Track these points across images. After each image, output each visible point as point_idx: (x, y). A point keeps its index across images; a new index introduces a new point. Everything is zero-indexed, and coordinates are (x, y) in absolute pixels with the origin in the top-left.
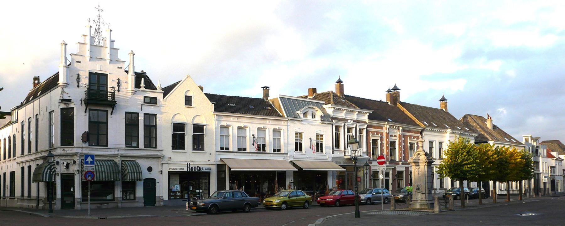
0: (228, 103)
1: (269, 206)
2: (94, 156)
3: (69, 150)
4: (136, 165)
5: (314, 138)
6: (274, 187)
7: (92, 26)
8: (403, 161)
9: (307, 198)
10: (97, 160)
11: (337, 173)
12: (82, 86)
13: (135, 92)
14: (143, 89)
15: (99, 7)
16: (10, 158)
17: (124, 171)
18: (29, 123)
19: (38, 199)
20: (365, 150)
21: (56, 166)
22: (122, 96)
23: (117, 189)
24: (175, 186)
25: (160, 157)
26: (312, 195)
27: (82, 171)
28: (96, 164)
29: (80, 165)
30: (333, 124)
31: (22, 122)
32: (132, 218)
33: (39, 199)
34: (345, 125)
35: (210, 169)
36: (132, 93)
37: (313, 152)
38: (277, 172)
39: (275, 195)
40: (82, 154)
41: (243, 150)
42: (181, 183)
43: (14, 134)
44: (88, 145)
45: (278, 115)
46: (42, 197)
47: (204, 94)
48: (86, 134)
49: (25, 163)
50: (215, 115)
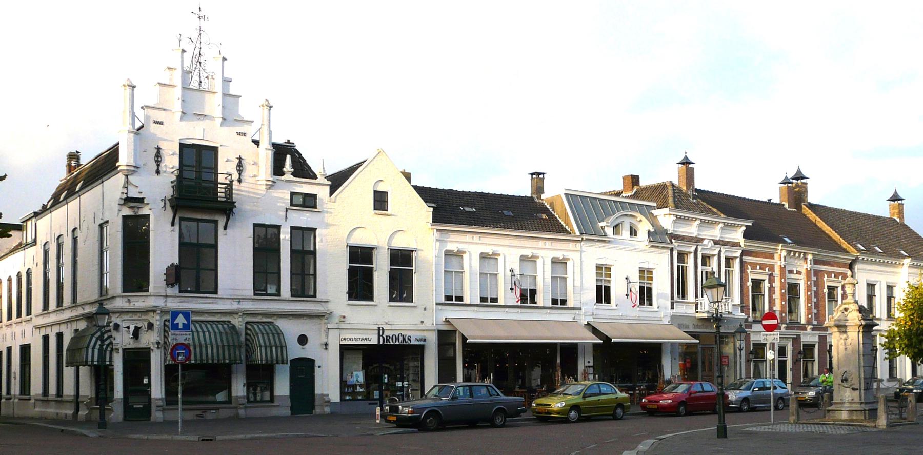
0: (461, 206)
1: (543, 415)
2: (189, 312)
3: (140, 302)
4: (274, 332)
5: (635, 277)
6: (553, 377)
7: (185, 49)
8: (815, 323)
9: (620, 398)
10: (197, 321)
11: (680, 347)
12: (165, 172)
13: (273, 184)
14: (288, 177)
15: (200, 11)
16: (21, 317)
17: (252, 344)
18: (59, 246)
19: (77, 401)
20: (737, 301)
21: (114, 334)
22: (246, 192)
23: (235, 380)
24: (355, 373)
25: (324, 316)
26: (630, 392)
27: (165, 343)
28: (194, 330)
29: (162, 331)
30: (672, 248)
31: (45, 245)
32: (266, 438)
33: (80, 399)
34: (696, 250)
35: (425, 340)
36: (266, 184)
37: (633, 305)
38: (560, 346)
39: (556, 392)
40: (166, 310)
41: (491, 302)
42: (364, 367)
43: (29, 269)
44: (178, 291)
45: (562, 230)
46: (84, 396)
47: (412, 188)
48: (174, 268)
49: (50, 327)
50: (435, 230)
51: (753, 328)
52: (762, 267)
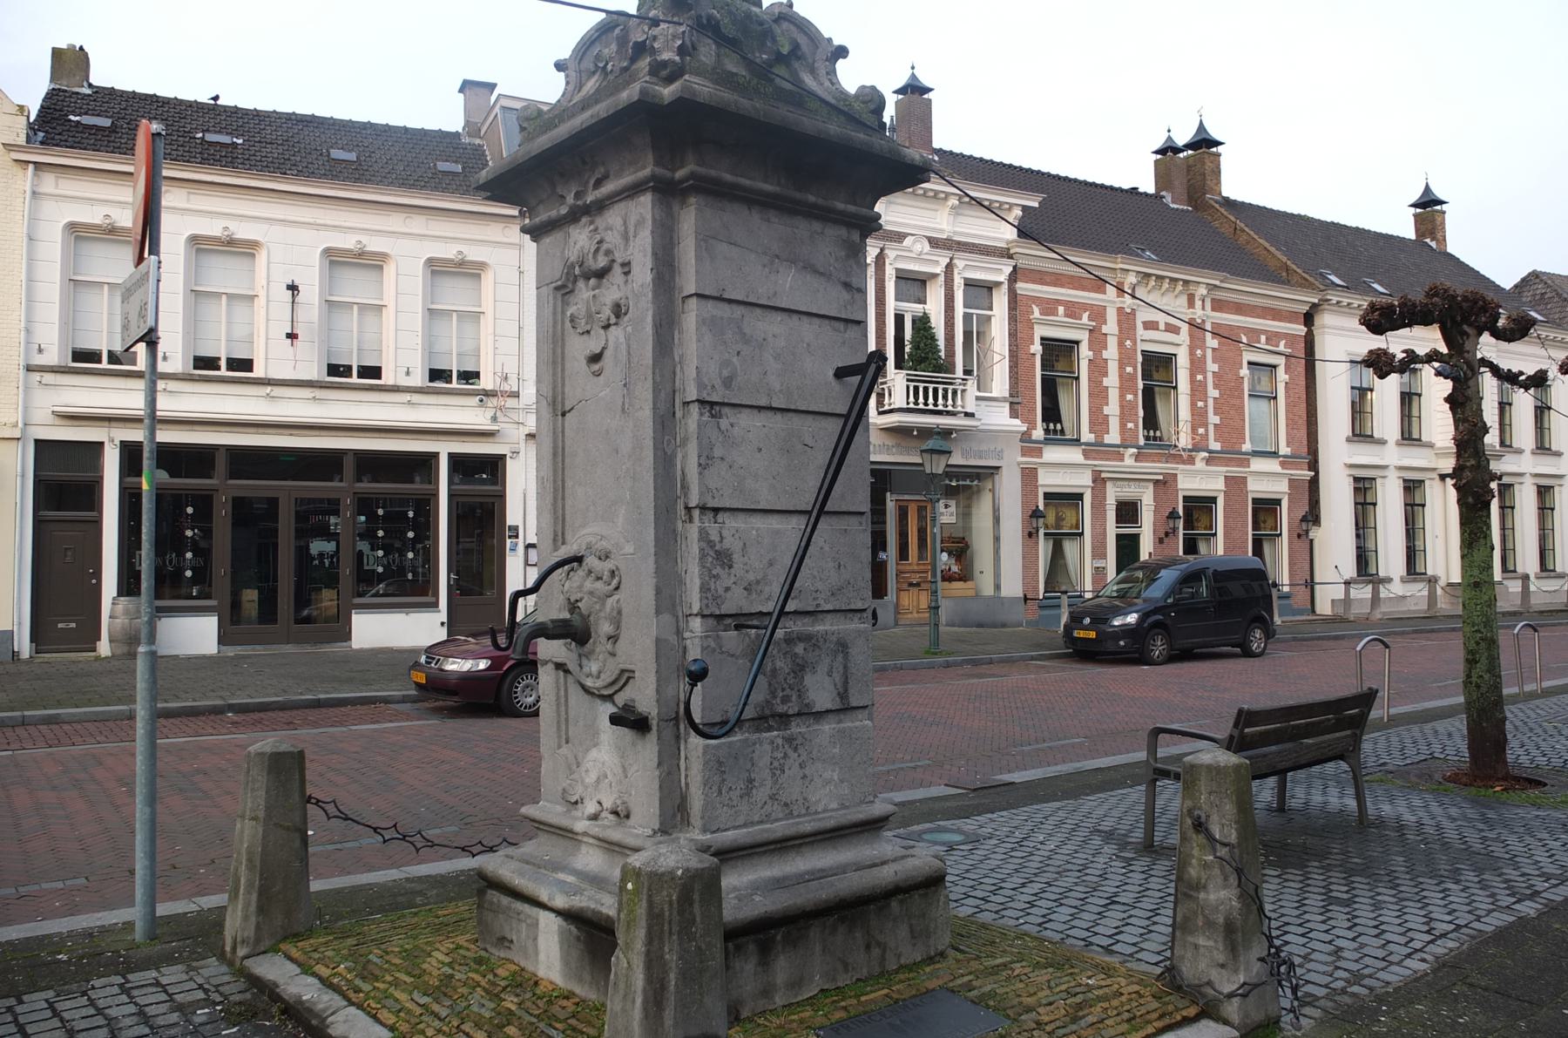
51: (1044, 455)
52: (1073, 310)
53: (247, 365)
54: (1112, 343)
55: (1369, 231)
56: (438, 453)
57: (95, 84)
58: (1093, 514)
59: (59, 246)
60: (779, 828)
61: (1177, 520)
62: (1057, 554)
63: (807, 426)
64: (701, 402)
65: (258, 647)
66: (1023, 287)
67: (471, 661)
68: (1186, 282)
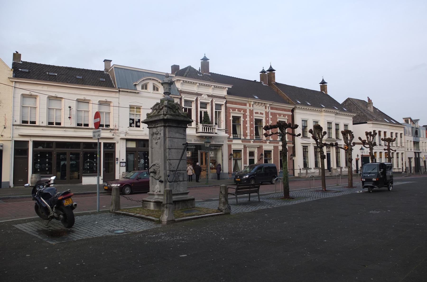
52: (239, 110)
53: (60, 124)
54: (248, 117)
55: (309, 90)
56: (101, 142)
57: (22, 61)
58: (244, 154)
59: (20, 99)
60: (177, 193)
61: (262, 156)
62: (236, 164)
63: (180, 150)
64: (169, 148)
65: (62, 185)
66: (228, 105)
67: (117, 184)
68: (264, 104)
